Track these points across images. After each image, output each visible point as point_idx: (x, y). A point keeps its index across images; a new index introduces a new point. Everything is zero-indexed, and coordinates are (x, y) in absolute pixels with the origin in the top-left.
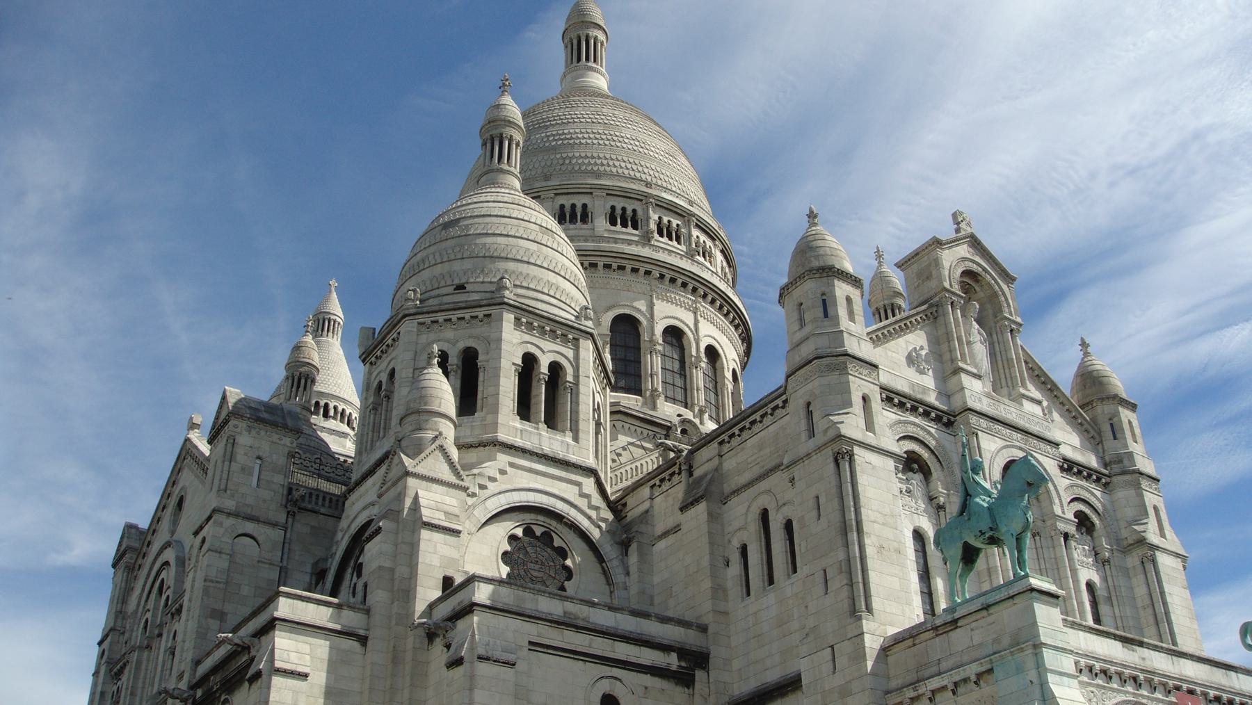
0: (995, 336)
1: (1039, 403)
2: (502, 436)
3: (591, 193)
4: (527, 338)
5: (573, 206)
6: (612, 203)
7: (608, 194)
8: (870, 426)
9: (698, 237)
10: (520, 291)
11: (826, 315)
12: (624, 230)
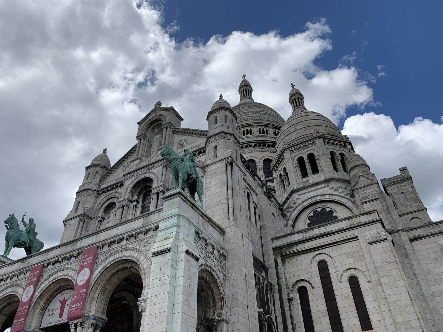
9: (244, 131)
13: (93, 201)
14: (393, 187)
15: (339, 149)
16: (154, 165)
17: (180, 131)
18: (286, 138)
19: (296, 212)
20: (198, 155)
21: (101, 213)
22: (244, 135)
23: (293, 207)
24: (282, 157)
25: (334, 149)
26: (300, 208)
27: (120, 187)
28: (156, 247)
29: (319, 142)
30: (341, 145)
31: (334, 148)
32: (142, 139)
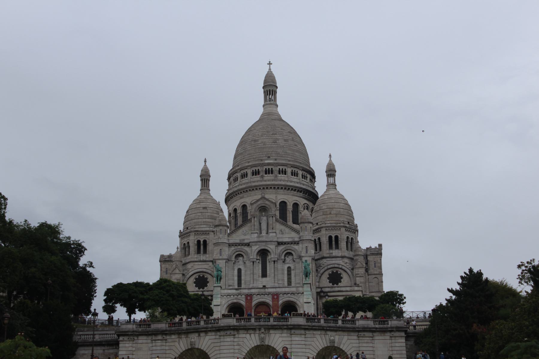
0: (269, 219)
1: (276, 232)
2: (192, 260)
3: (247, 168)
4: (198, 237)
5: (244, 172)
6: (252, 169)
7: (251, 167)
8: (221, 255)
9: (279, 169)
10: (197, 226)
11: (216, 235)
12: (256, 176)
13: (228, 250)
14: (371, 256)
15: (351, 234)
16: (269, 243)
17: (281, 222)
18: (324, 216)
19: (323, 270)
20: (294, 244)
21: (233, 258)
22: (279, 173)
23: (322, 267)
24: (320, 230)
25: (349, 235)
26: (326, 268)
27: (244, 246)
28: (305, 300)
29: (343, 229)
30: (353, 231)
31: (349, 233)
32: (255, 217)
